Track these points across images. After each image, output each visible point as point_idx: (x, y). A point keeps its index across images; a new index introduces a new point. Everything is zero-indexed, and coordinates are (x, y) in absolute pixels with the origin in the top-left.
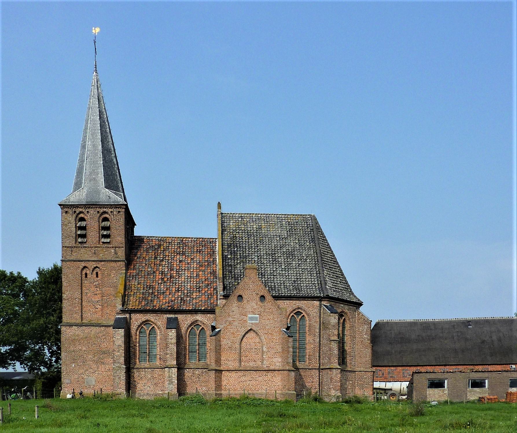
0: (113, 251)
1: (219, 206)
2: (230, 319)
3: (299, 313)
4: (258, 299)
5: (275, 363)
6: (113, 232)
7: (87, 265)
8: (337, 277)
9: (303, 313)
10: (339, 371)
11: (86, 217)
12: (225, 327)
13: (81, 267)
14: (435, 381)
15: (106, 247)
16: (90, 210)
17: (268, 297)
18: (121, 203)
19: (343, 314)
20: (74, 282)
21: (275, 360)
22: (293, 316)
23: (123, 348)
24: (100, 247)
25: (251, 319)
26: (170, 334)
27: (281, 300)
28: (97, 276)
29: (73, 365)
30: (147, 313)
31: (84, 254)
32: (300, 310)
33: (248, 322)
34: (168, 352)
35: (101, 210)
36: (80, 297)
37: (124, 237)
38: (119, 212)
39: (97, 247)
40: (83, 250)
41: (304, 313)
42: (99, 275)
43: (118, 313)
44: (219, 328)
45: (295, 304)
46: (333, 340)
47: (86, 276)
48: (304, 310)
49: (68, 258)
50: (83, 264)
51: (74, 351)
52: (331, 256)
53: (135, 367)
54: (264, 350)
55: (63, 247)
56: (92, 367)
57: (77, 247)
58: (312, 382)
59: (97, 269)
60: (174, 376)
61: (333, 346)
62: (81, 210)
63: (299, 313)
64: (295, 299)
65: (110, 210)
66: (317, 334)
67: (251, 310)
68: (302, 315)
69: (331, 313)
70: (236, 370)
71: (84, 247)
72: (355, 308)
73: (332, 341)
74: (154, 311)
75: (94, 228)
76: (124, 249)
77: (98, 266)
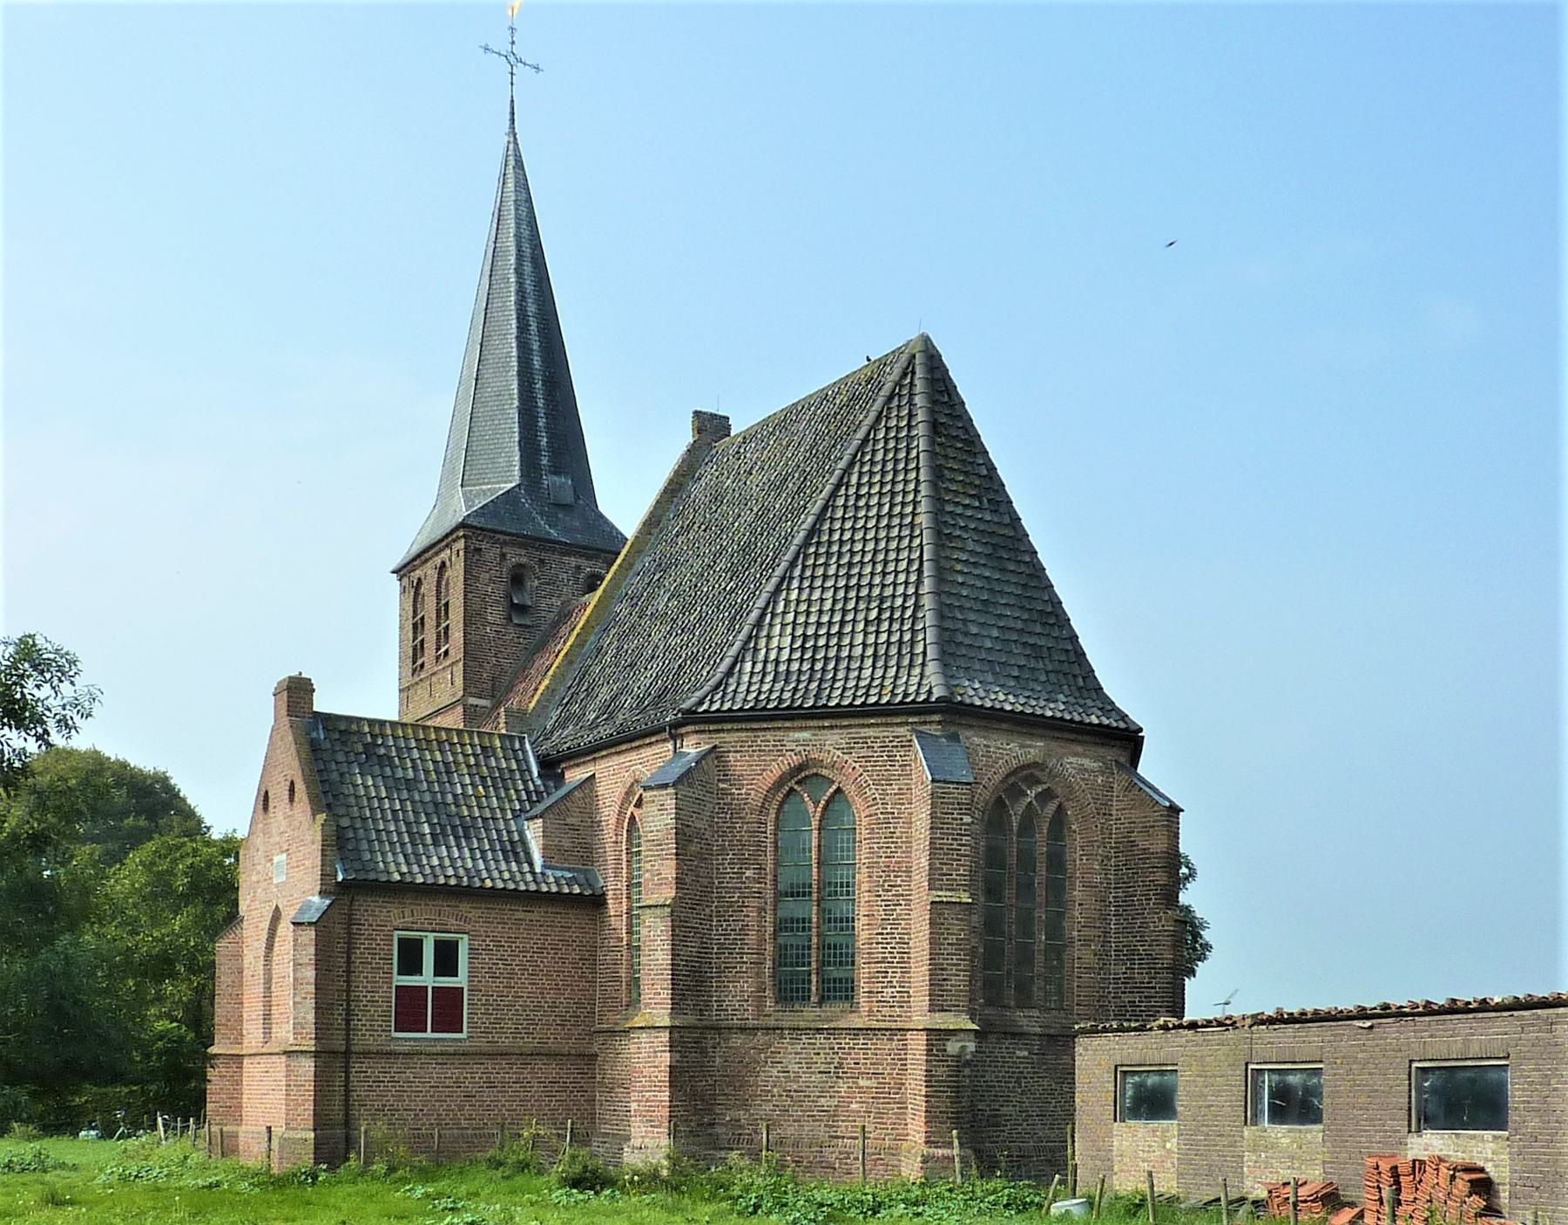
10: (665, 1037)
19: (825, 772)
35: (438, 561)
46: (649, 907)
53: (638, 1021)
55: (400, 691)
61: (652, 933)
64: (604, 753)
72: (902, 730)
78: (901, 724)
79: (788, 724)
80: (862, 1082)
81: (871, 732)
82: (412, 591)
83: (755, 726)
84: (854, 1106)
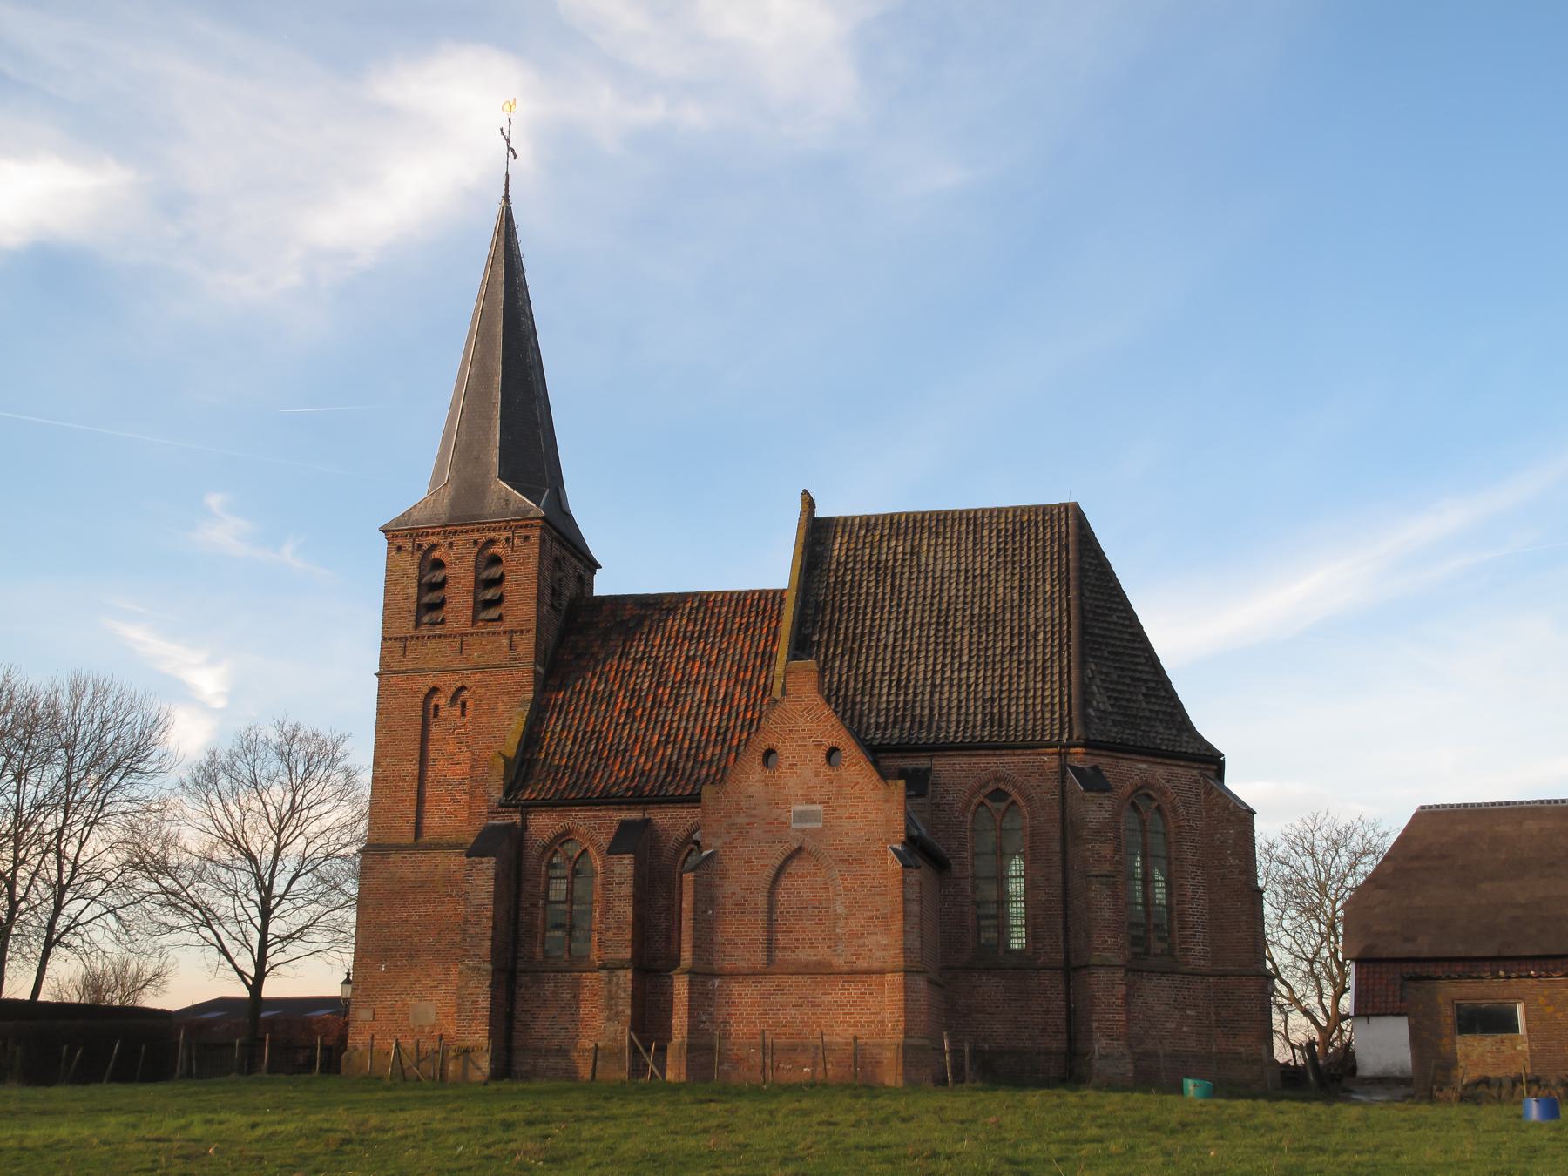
0: (505, 642)
1: (808, 502)
2: (741, 820)
3: (998, 795)
4: (821, 758)
5: (871, 950)
6: (508, 588)
7: (439, 684)
8: (1132, 679)
9: (1010, 795)
11: (446, 560)
12: (725, 843)
13: (426, 690)
14: (1483, 1006)
15: (488, 633)
16: (454, 539)
17: (851, 751)
18: (532, 514)
21: (871, 941)
22: (982, 803)
23: (490, 914)
24: (472, 635)
25: (802, 817)
26: (618, 869)
27: (945, 756)
28: (463, 714)
30: (570, 811)
31: (435, 653)
32: (1002, 786)
33: (793, 826)
34: (612, 922)
36: (416, 773)
37: (534, 603)
38: (526, 538)
39: (466, 634)
40: (432, 645)
41: (1015, 795)
42: (470, 713)
43: (492, 813)
44: (709, 847)
45: (985, 769)
46: (1097, 876)
47: (436, 716)
48: (1015, 786)
49: (395, 666)
52: (1124, 618)
54: (839, 911)
55: (384, 639)
57: (418, 638)
58: (1047, 1012)
59: (465, 695)
60: (623, 995)
62: (433, 539)
63: (998, 795)
65: (506, 534)
66: (1057, 859)
67: (800, 792)
68: (1010, 799)
69: (1087, 789)
70: (754, 974)
73: (1095, 879)
74: (586, 802)
76: (532, 635)
77: (467, 684)
78: (1194, 768)
79: (1138, 758)
80: (1189, 1012)
81: (1180, 770)
82: (418, 555)
83: (1120, 755)
84: (1185, 1029)
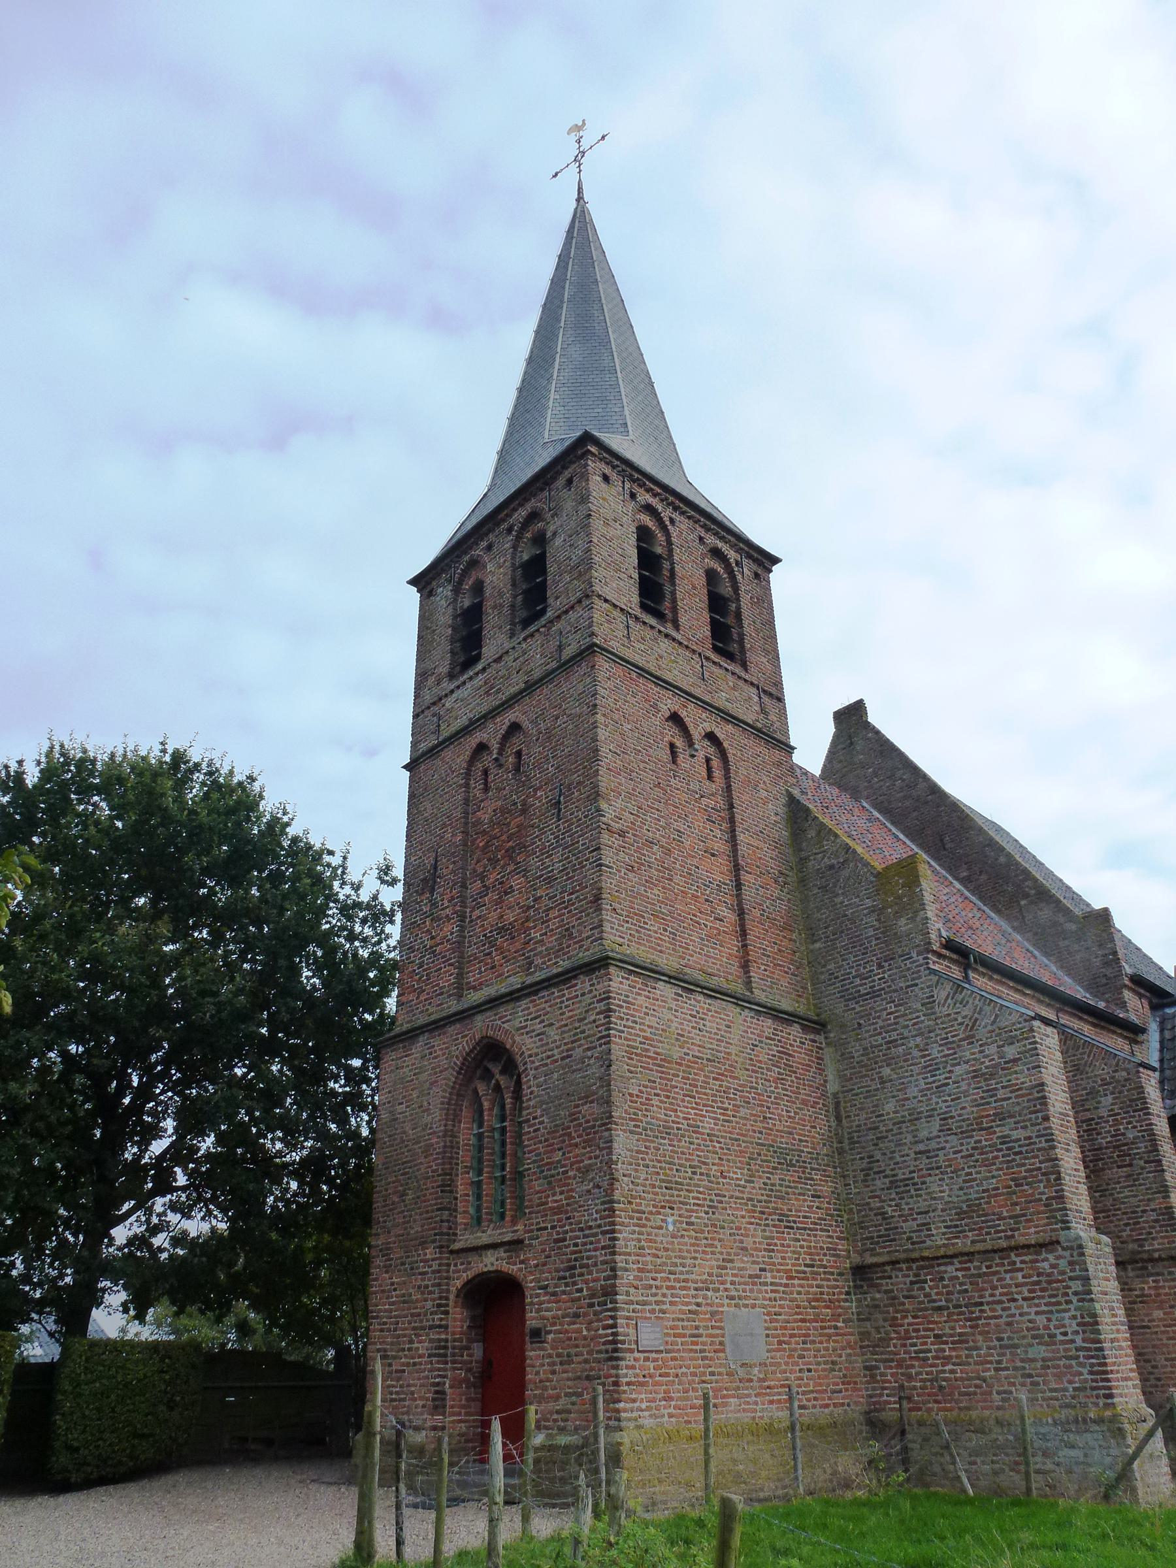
0: (756, 699)
7: (683, 714)
20: (642, 765)
24: (714, 663)
28: (710, 777)
29: (670, 1220)
40: (665, 645)
50: (669, 703)
51: (666, 1131)
56: (748, 1242)
71: (667, 636)
75: (694, 588)
